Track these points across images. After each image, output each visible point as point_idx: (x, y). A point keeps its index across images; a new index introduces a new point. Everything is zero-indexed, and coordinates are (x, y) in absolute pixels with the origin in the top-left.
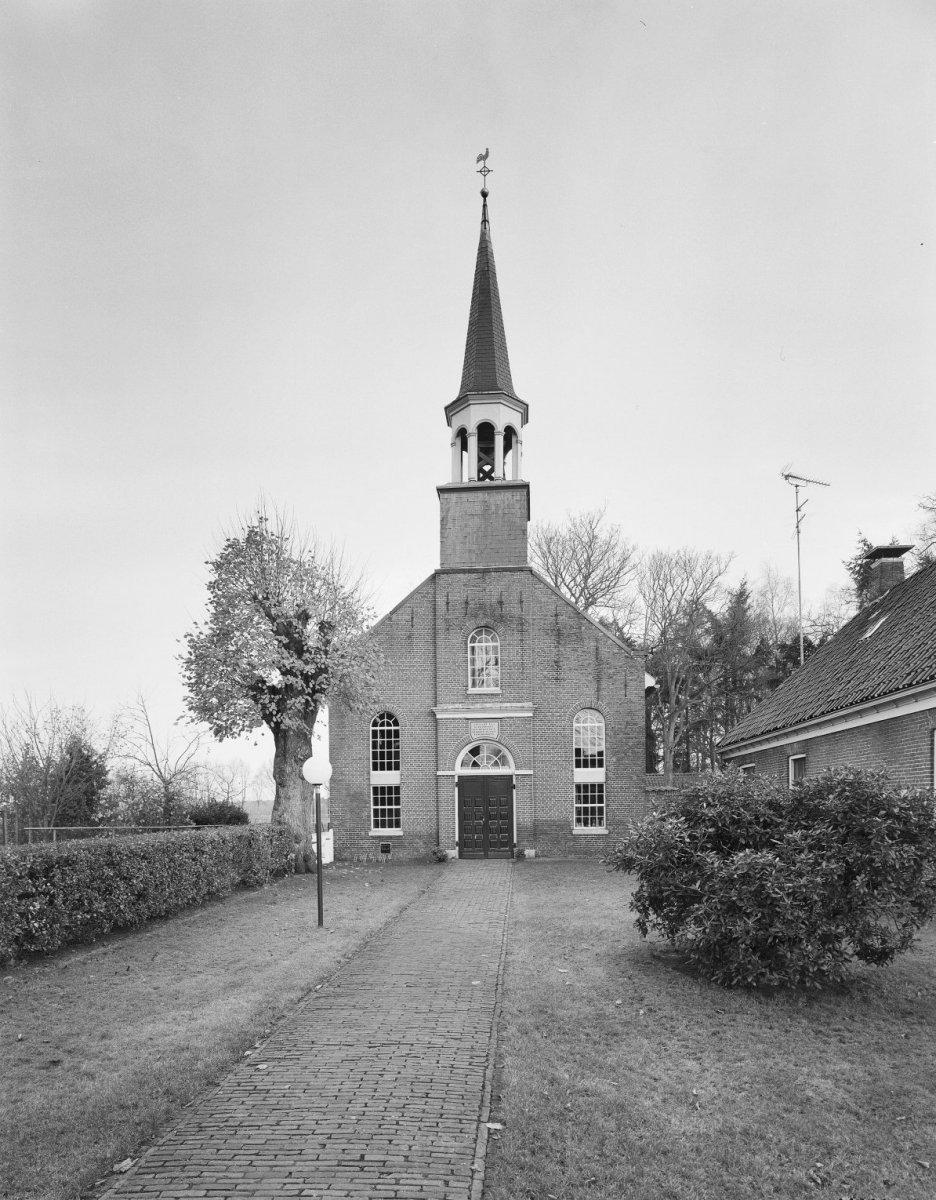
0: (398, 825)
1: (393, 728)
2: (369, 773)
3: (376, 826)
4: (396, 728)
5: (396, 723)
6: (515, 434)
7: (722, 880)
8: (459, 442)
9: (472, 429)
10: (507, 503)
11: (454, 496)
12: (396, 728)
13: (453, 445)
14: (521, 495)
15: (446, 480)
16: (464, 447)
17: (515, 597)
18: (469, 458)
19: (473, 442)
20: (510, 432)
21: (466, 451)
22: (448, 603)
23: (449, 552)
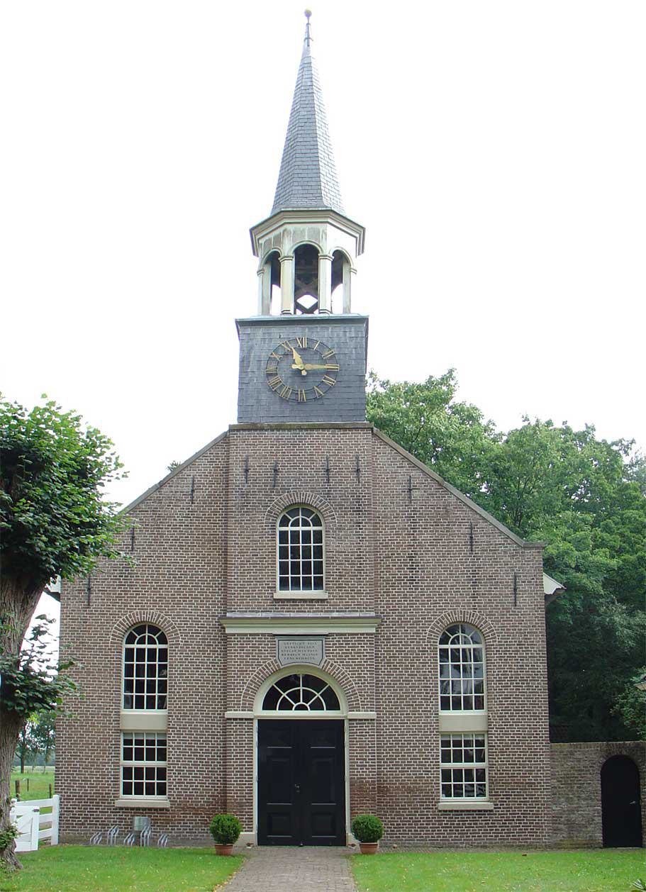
0: (162, 791)
1: (158, 646)
2: (118, 713)
3: (127, 790)
4: (163, 646)
5: (163, 640)
6: (348, 261)
7: (634, 709)
8: (268, 270)
9: (287, 248)
10: (336, 340)
11: (260, 332)
12: (163, 646)
13: (260, 272)
14: (357, 332)
15: (253, 313)
16: (276, 278)
17: (349, 463)
18: (282, 294)
19: (288, 269)
20: (340, 259)
21: (279, 285)
22: (247, 471)
23: (252, 401)
